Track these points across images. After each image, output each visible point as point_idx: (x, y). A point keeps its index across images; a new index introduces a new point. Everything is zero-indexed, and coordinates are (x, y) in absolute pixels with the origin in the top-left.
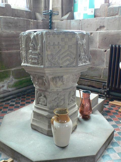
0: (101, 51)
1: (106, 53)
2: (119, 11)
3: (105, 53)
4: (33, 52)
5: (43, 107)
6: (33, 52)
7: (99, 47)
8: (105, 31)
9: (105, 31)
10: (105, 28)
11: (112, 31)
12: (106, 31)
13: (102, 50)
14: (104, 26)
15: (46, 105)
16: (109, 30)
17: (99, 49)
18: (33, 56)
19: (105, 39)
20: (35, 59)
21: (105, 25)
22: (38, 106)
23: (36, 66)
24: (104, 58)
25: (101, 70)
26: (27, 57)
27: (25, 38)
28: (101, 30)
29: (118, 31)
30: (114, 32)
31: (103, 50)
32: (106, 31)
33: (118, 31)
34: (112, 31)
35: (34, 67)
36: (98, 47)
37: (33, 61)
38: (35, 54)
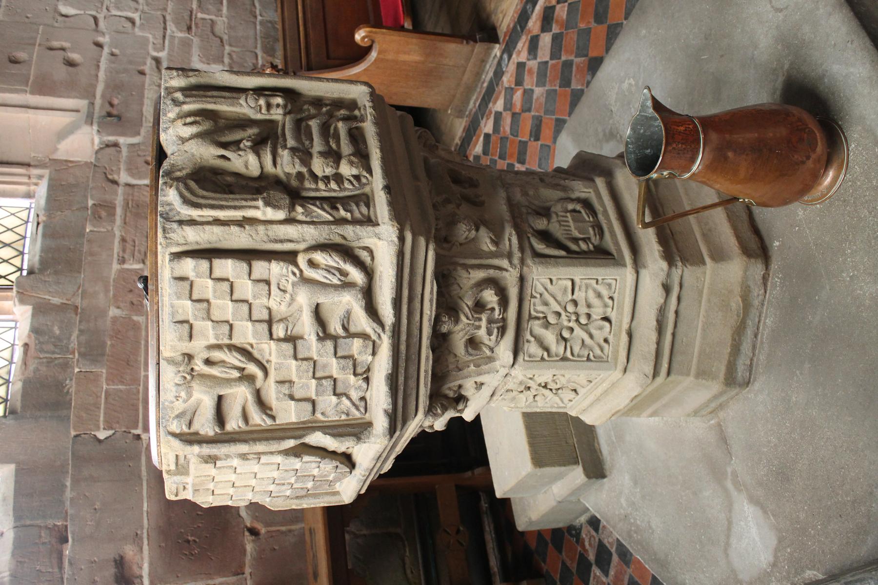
0: (260, 559)
1: (267, 525)
2: (39, 522)
3: (263, 531)
4: (291, 143)
5: (605, 212)
6: (291, 143)
7: (236, 574)
8: (146, 547)
9: (146, 547)
10: (129, 551)
11: (145, 508)
12: (146, 542)
13: (248, 558)
14: (115, 561)
15: (587, 204)
16: (142, 528)
17: (248, 570)
18: (318, 146)
19: (188, 541)
20: (326, 131)
21: (109, 552)
22: (617, 244)
23: (369, 129)
24: (290, 531)
25: (359, 541)
26: (332, 203)
27: (203, 197)
28: (141, 577)
29: (145, 479)
30: (149, 497)
31: (249, 547)
32: (146, 542)
33: (145, 479)
34: (145, 508)
35: (382, 150)
36: (235, 578)
37: (346, 148)
38: (300, 128)
